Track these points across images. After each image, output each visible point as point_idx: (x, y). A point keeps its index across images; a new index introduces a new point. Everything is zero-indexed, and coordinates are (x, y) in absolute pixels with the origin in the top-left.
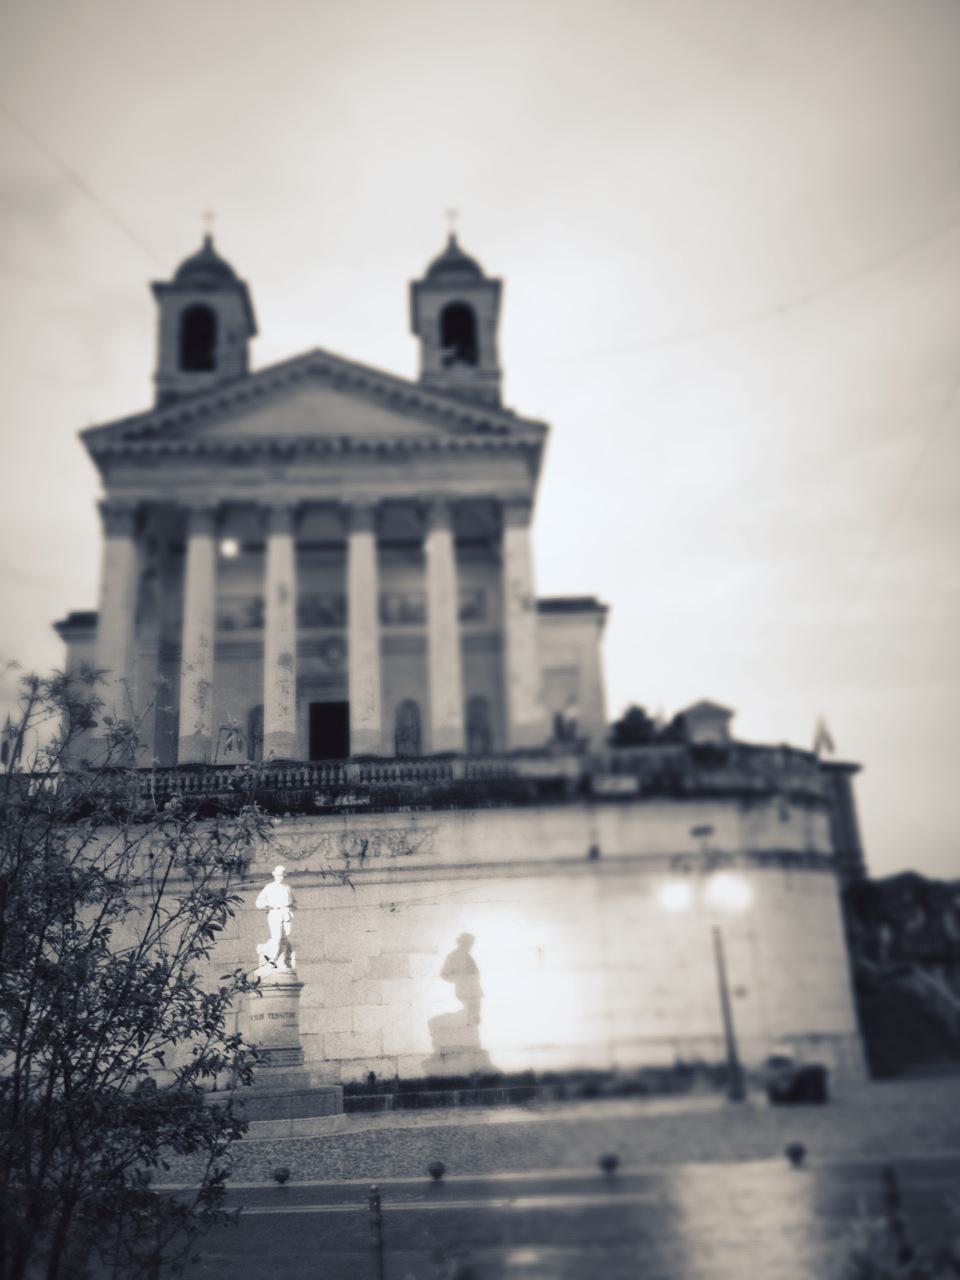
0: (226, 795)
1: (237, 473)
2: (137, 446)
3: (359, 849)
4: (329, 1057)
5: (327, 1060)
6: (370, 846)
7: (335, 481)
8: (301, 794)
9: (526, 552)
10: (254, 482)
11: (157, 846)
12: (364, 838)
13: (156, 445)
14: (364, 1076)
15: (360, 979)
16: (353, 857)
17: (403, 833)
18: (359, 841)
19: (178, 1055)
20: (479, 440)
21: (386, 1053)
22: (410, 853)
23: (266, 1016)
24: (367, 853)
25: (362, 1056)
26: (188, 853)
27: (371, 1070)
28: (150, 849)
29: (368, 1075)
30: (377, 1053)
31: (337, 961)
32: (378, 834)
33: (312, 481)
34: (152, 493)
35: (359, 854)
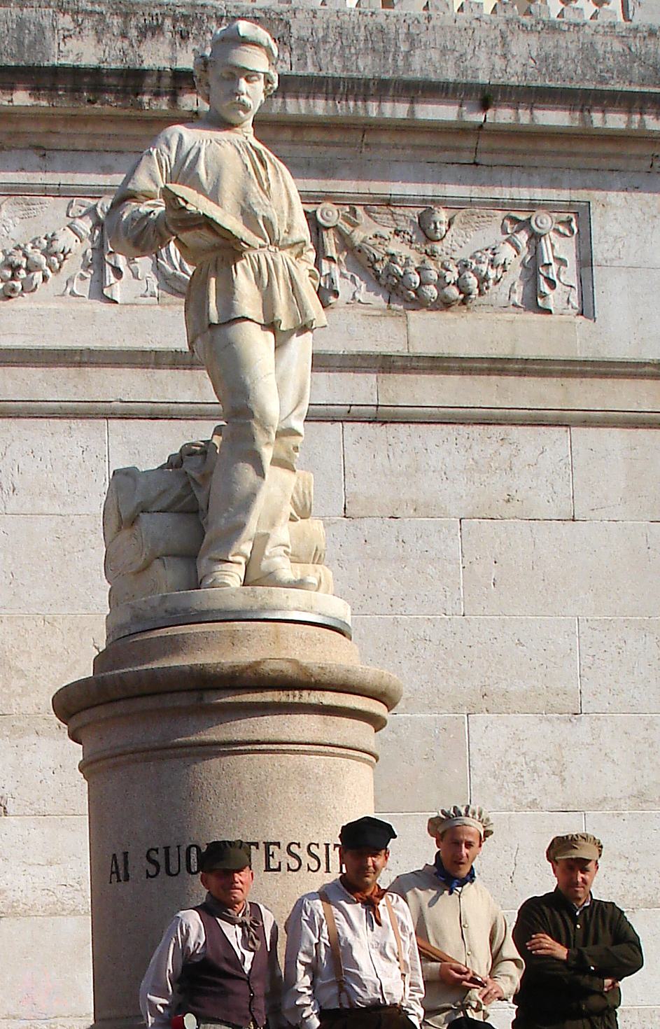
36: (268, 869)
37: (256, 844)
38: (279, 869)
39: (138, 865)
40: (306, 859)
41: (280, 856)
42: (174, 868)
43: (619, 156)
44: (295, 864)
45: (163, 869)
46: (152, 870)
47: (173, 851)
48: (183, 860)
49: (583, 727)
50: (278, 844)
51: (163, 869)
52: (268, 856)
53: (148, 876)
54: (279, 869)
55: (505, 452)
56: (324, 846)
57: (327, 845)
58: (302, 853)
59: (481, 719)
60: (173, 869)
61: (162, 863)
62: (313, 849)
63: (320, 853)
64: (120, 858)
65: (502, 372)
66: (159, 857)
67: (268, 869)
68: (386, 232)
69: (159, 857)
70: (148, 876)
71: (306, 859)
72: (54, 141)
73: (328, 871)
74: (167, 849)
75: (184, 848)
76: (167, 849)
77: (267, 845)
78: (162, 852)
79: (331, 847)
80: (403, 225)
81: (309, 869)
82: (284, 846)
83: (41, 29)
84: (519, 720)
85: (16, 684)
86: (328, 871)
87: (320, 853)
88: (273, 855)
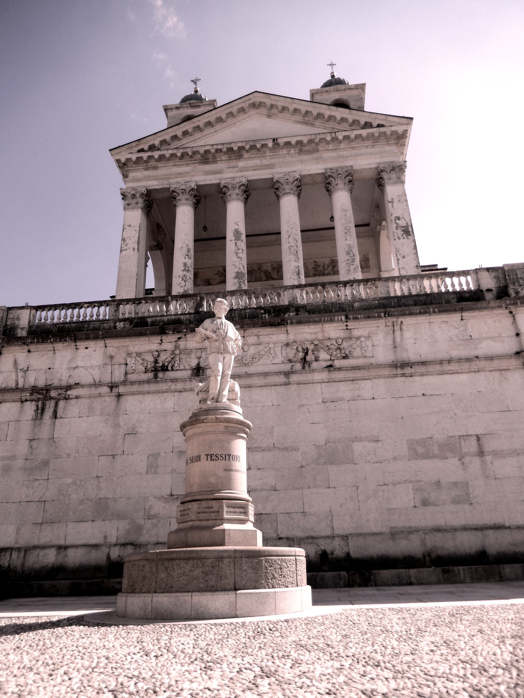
0: (187, 316)
1: (207, 167)
2: (145, 155)
3: (301, 355)
4: (281, 536)
5: (281, 538)
6: (310, 352)
7: (271, 166)
8: (249, 313)
9: (403, 199)
10: (220, 172)
11: (131, 356)
12: (304, 347)
13: (156, 154)
14: (316, 552)
15: (308, 465)
16: (295, 362)
17: (340, 341)
18: (300, 349)
19: (144, 531)
20: (364, 132)
21: (336, 532)
22: (346, 357)
23: (203, 457)
24: (308, 358)
25: (313, 534)
26: (156, 362)
27: (323, 548)
28: (125, 359)
29: (320, 552)
30: (328, 532)
31: (286, 449)
32: (316, 342)
33: (255, 169)
34: (154, 185)
35: (301, 359)
39: (189, 461)
40: (220, 458)
41: (214, 457)
43: (378, 323)
44: (217, 459)
49: (380, 444)
52: (211, 457)
55: (357, 386)
58: (219, 456)
59: (356, 443)
63: (224, 456)
65: (355, 369)
66: (191, 459)
68: (329, 344)
69: (191, 459)
71: (220, 458)
72: (260, 333)
77: (211, 455)
80: (332, 343)
83: (257, 313)
84: (365, 443)
85: (253, 441)
87: (224, 456)
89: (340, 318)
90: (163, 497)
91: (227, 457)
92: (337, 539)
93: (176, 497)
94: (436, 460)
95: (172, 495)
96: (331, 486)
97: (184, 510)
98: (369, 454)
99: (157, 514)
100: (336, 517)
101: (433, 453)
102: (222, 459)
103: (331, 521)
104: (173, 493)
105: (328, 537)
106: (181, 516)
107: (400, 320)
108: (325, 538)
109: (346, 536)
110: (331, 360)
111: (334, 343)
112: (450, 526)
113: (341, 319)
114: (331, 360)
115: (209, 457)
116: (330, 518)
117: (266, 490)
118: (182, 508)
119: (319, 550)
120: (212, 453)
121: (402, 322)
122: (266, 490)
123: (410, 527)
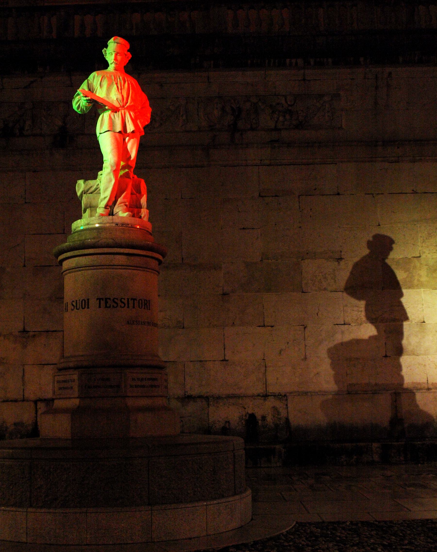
4: (190, 393)
21: (271, 390)
22: (300, 126)
25: (237, 392)
27: (250, 412)
30: (259, 389)
36: (106, 307)
37: (102, 299)
38: (110, 307)
42: (78, 306)
44: (115, 305)
45: (75, 308)
46: (73, 307)
47: (78, 301)
48: (80, 305)
50: (110, 299)
51: (75, 308)
52: (106, 302)
53: (72, 310)
54: (110, 307)
56: (127, 300)
57: (128, 299)
58: (119, 302)
60: (78, 308)
61: (75, 306)
62: (123, 300)
63: (126, 301)
64: (66, 304)
66: (74, 304)
67: (106, 307)
69: (74, 304)
70: (72, 310)
73: (128, 307)
74: (76, 301)
75: (81, 301)
76: (76, 301)
77: (106, 299)
78: (75, 302)
79: (130, 300)
81: (121, 307)
82: (112, 299)
86: (128, 307)
87: (126, 301)
88: (108, 302)
89: (294, 61)
90: (11, 334)
91: (131, 302)
92: (271, 399)
93: (31, 334)
94: (422, 290)
95: (24, 331)
96: (265, 325)
97: (65, 381)
98: (325, 278)
99: (3, 359)
100: (271, 369)
101: (418, 280)
102: (123, 305)
103: (265, 373)
104: (28, 329)
105: (258, 395)
106: (60, 389)
107: (388, 69)
108: (253, 397)
109: (285, 395)
110: (276, 129)
111: (283, 102)
112: (433, 384)
113: (296, 63)
114: (276, 129)
115: (103, 303)
116: (263, 369)
117: (169, 327)
118: (61, 378)
119: (244, 413)
120: (108, 296)
121: (390, 73)
122: (169, 327)
123: (376, 385)
